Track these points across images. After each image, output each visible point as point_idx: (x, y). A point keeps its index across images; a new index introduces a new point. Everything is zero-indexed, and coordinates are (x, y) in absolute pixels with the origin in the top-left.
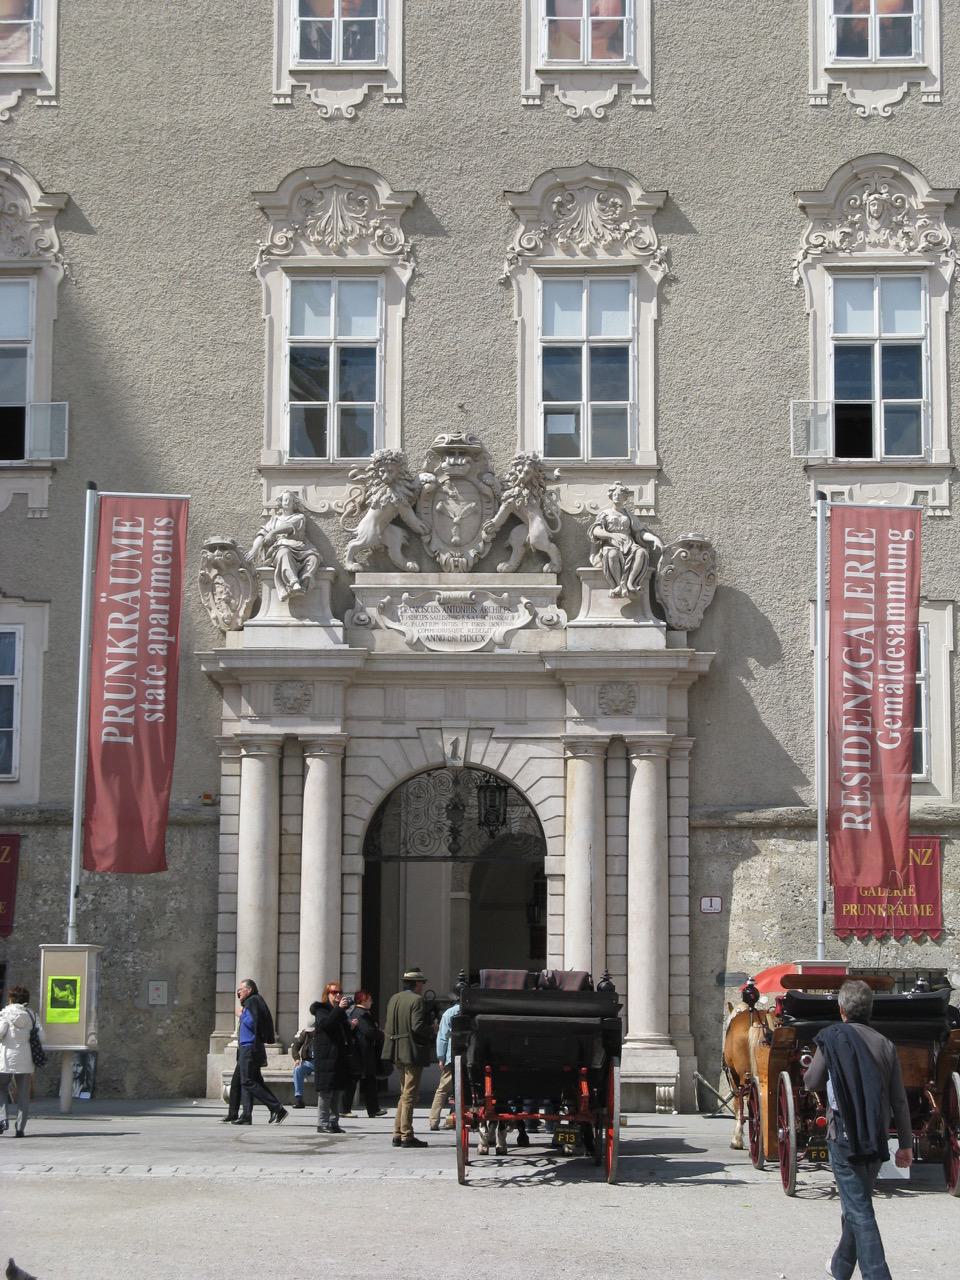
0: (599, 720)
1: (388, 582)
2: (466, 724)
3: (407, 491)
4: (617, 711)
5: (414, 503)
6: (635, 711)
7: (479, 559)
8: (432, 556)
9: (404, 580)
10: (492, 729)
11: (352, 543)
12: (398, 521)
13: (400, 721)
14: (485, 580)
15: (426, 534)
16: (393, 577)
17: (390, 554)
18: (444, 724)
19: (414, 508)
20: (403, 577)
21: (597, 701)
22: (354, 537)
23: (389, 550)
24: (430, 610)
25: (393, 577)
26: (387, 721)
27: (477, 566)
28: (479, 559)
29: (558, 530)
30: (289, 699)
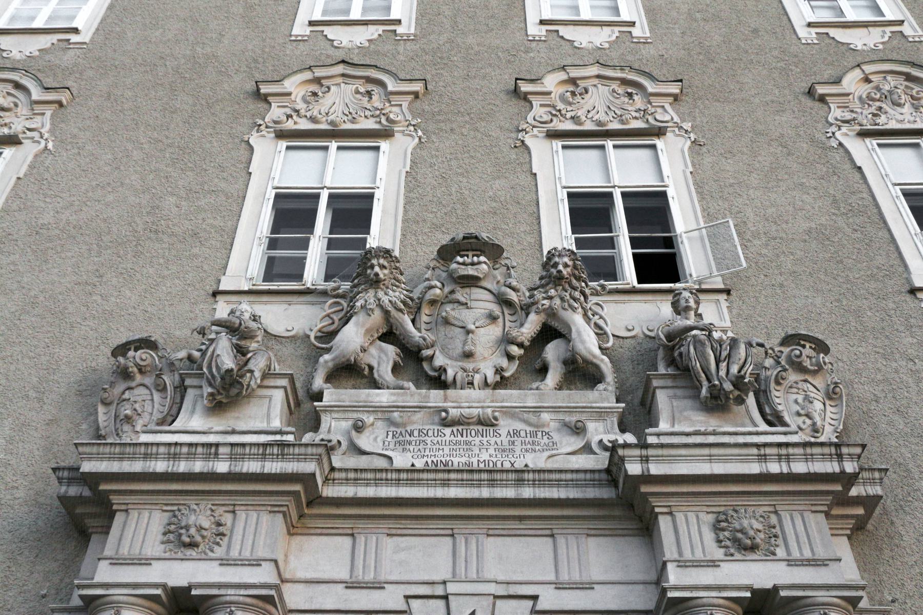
0: (722, 564)
1: (370, 399)
2: (492, 589)
3: (402, 296)
4: (753, 548)
5: (412, 317)
6: (781, 552)
7: (502, 378)
8: (436, 374)
9: (393, 398)
10: (535, 598)
11: (327, 357)
12: (390, 335)
13: (378, 586)
14: (511, 397)
15: (428, 348)
16: (378, 395)
17: (376, 375)
18: (452, 588)
19: (413, 321)
20: (394, 394)
21: (713, 535)
22: (328, 350)
23: (375, 371)
24: (430, 433)
25: (378, 395)
26: (352, 585)
27: (503, 382)
28: (502, 378)
29: (610, 344)
30: (187, 528)
